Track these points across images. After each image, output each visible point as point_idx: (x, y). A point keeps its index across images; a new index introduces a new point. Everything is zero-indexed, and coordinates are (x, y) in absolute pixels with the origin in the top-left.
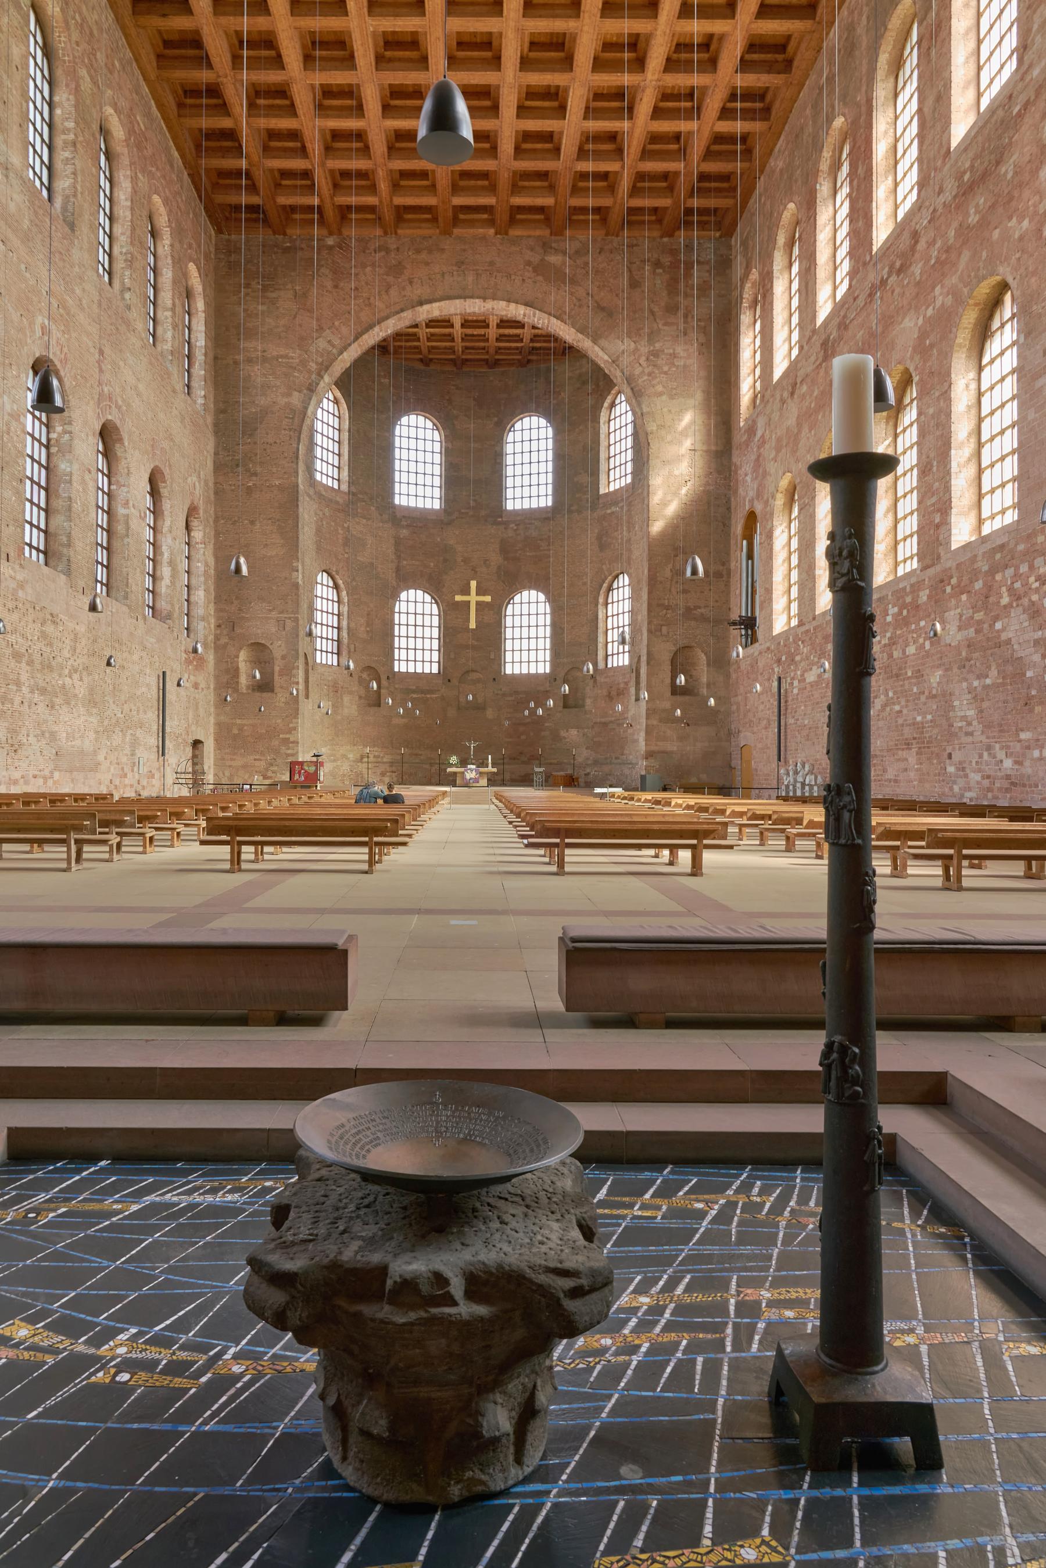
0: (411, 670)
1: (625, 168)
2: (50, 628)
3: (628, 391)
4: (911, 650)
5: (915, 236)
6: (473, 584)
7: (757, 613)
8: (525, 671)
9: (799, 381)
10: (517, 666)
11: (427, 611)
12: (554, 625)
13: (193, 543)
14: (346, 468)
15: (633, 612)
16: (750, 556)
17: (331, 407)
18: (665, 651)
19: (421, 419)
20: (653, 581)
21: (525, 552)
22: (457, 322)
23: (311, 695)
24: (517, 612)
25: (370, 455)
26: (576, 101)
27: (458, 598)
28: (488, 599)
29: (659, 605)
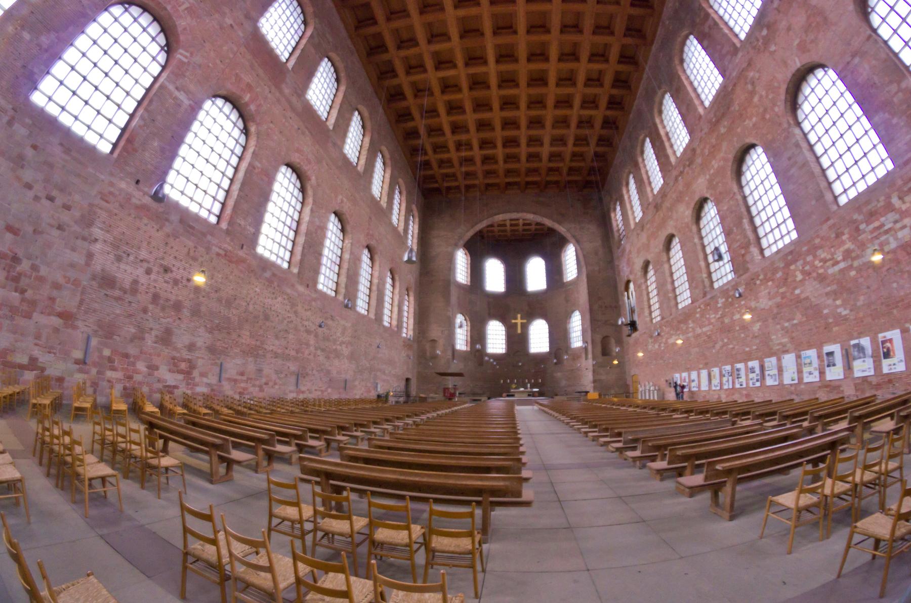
1: (564, 166)
3: (573, 240)
6: (519, 316)
7: (636, 318)
15: (582, 324)
16: (628, 298)
18: (598, 338)
20: (591, 311)
21: (536, 306)
22: (508, 223)
25: (477, 272)
26: (547, 140)
27: (513, 321)
28: (525, 321)
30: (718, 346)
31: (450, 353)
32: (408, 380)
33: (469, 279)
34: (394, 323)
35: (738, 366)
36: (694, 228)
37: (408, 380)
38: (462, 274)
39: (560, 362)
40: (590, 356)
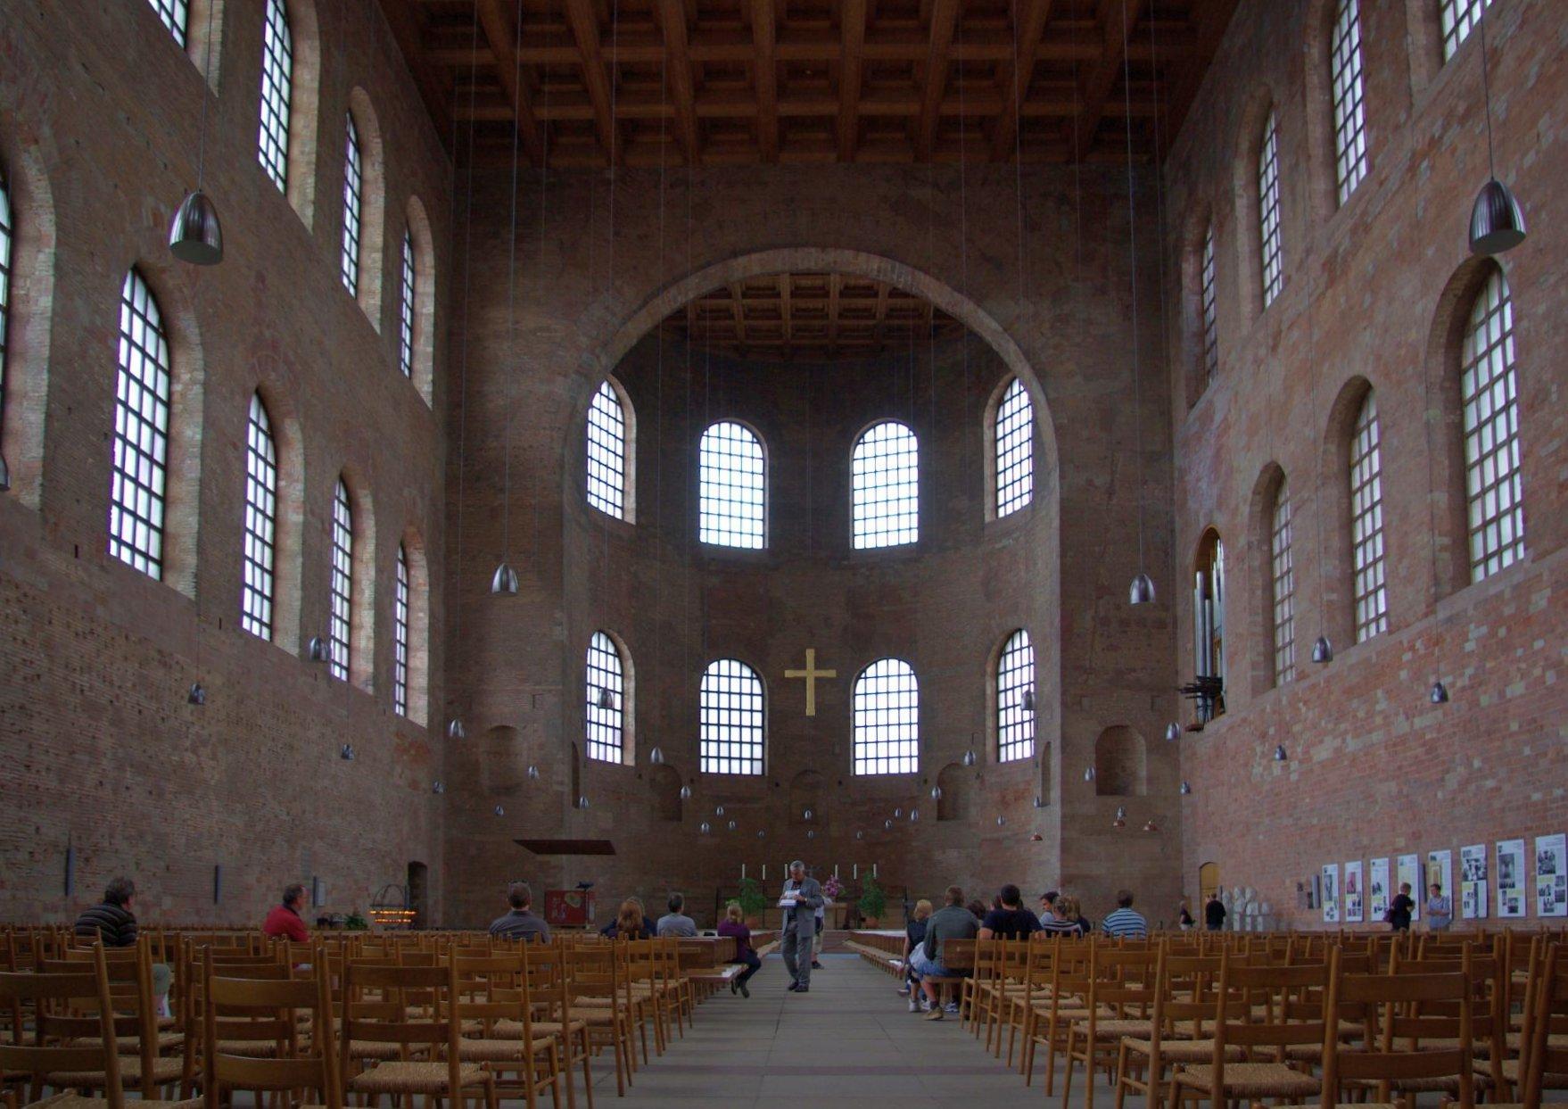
0: (724, 770)
2: (158, 674)
4: (1517, 688)
5: (1492, 57)
8: (883, 770)
9: (1284, 327)
10: (872, 764)
11: (746, 689)
12: (923, 706)
14: (633, 492)
17: (612, 408)
19: (736, 428)
24: (871, 689)
30: (1452, 781)
33: (631, 503)
35: (1508, 847)
36: (1438, 366)
38: (608, 485)
39: (947, 810)
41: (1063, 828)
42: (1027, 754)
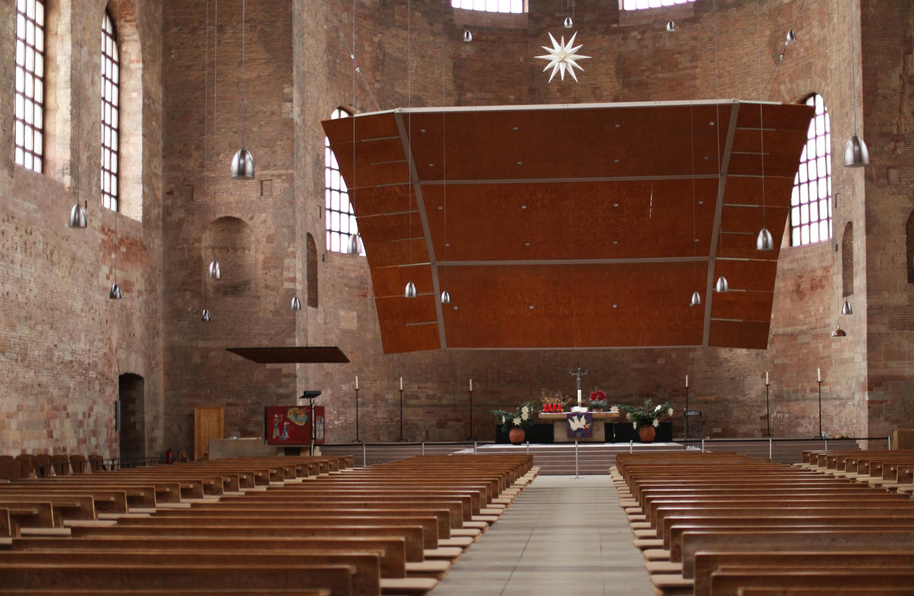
13: (125, 63)
23: (322, 299)
29: (883, 135)
31: (298, 268)
32: (129, 382)
34: (60, 154)
37: (129, 382)
40: (860, 281)
41: (870, 322)
42: (824, 237)
